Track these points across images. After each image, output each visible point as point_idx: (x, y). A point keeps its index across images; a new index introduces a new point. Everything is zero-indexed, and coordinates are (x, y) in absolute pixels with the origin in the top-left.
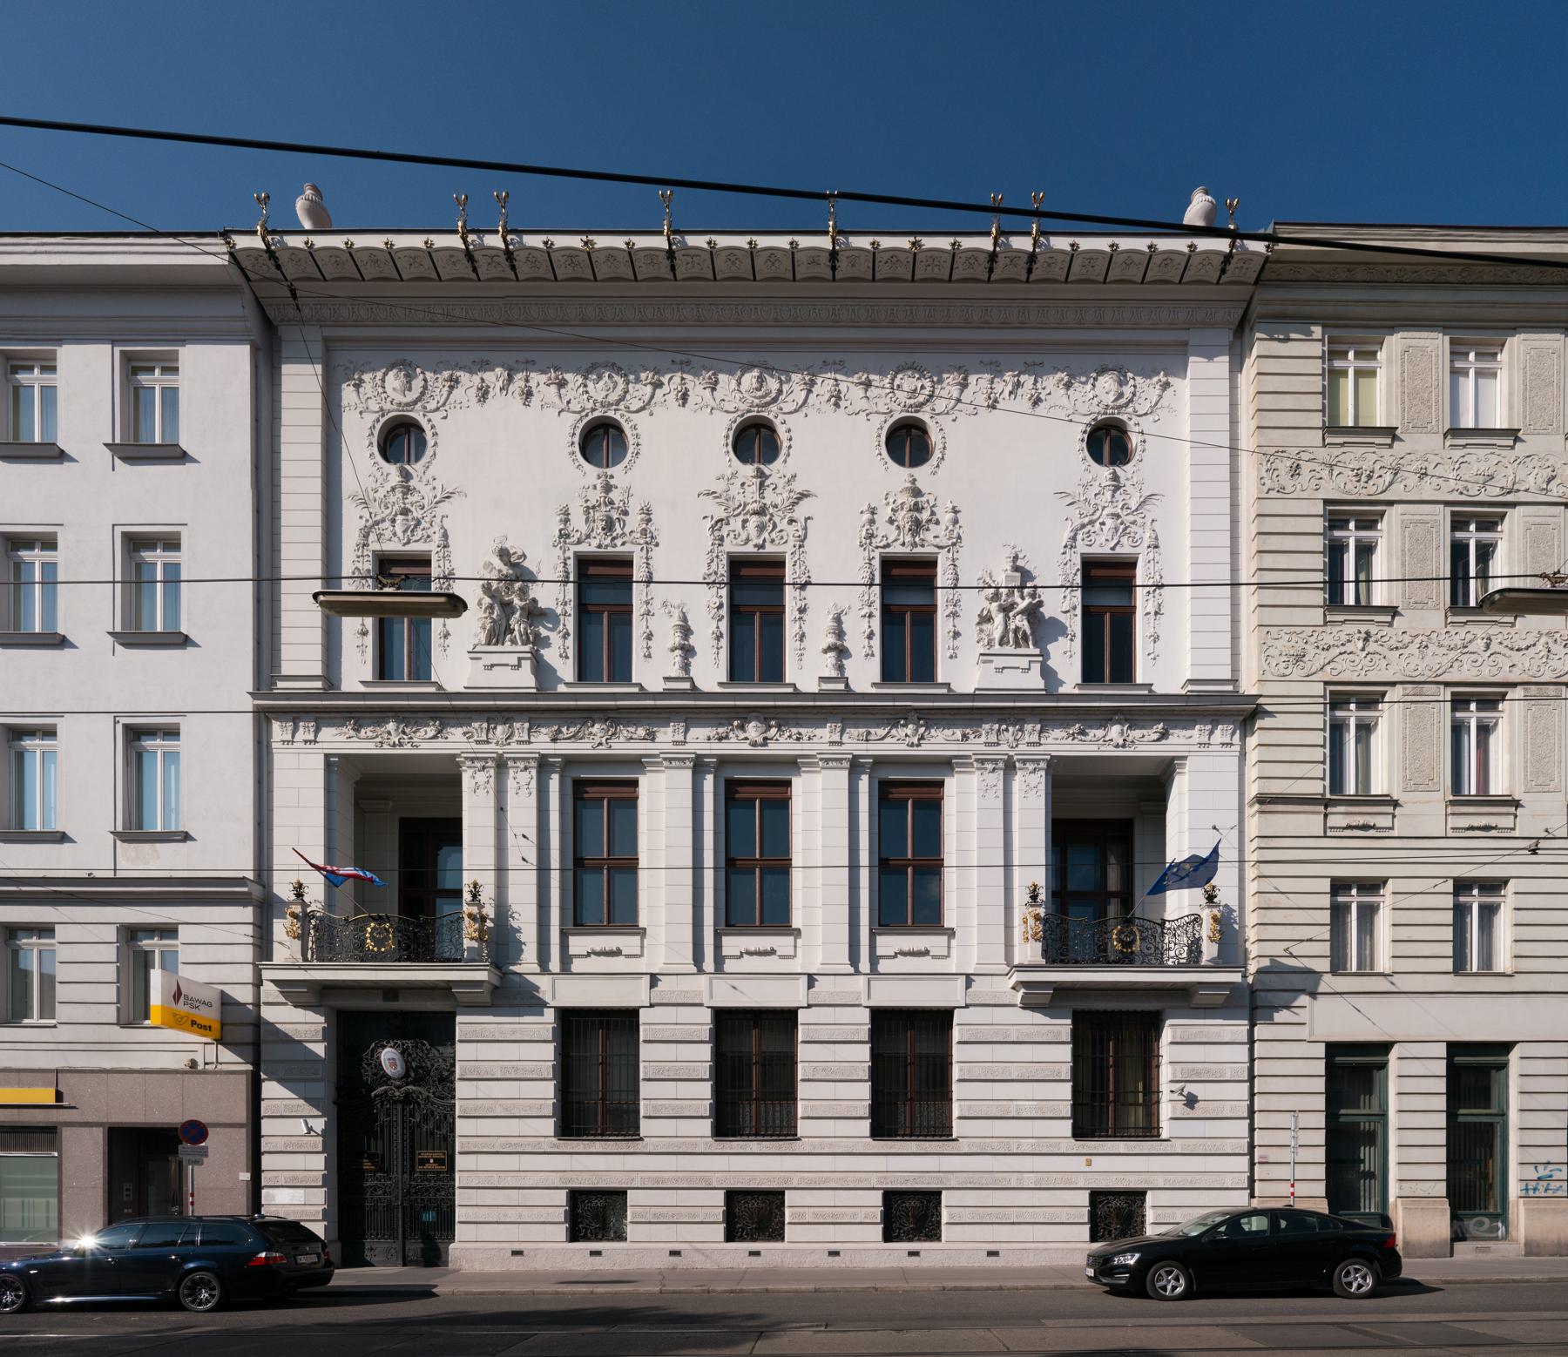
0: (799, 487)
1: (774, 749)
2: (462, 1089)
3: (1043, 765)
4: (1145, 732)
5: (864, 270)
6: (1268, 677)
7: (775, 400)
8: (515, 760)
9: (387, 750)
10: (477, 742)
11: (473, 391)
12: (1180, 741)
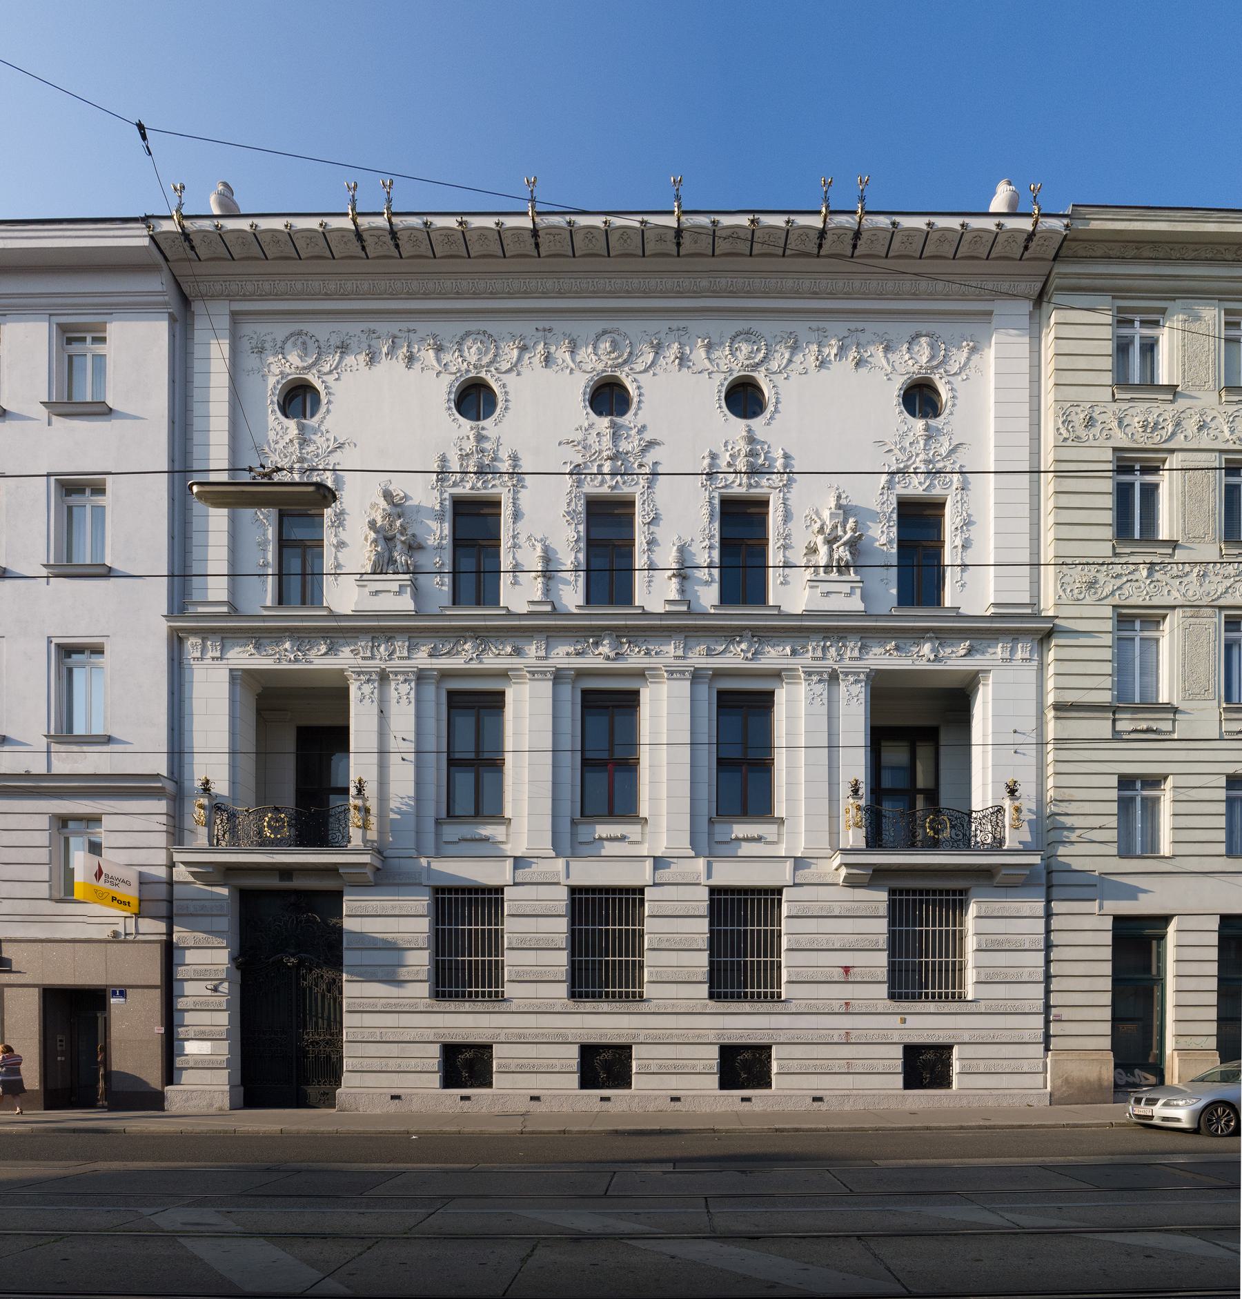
0: (648, 436)
3: (862, 677)
5: (704, 244)
6: (1064, 600)
8: (396, 674)
9: (285, 666)
10: (364, 658)
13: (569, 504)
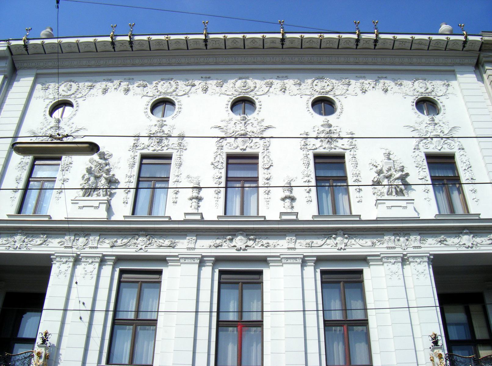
0: (265, 124)
3: (426, 259)
4: (482, 239)
7: (252, 91)
10: (66, 247)
11: (101, 90)
13: (215, 158)
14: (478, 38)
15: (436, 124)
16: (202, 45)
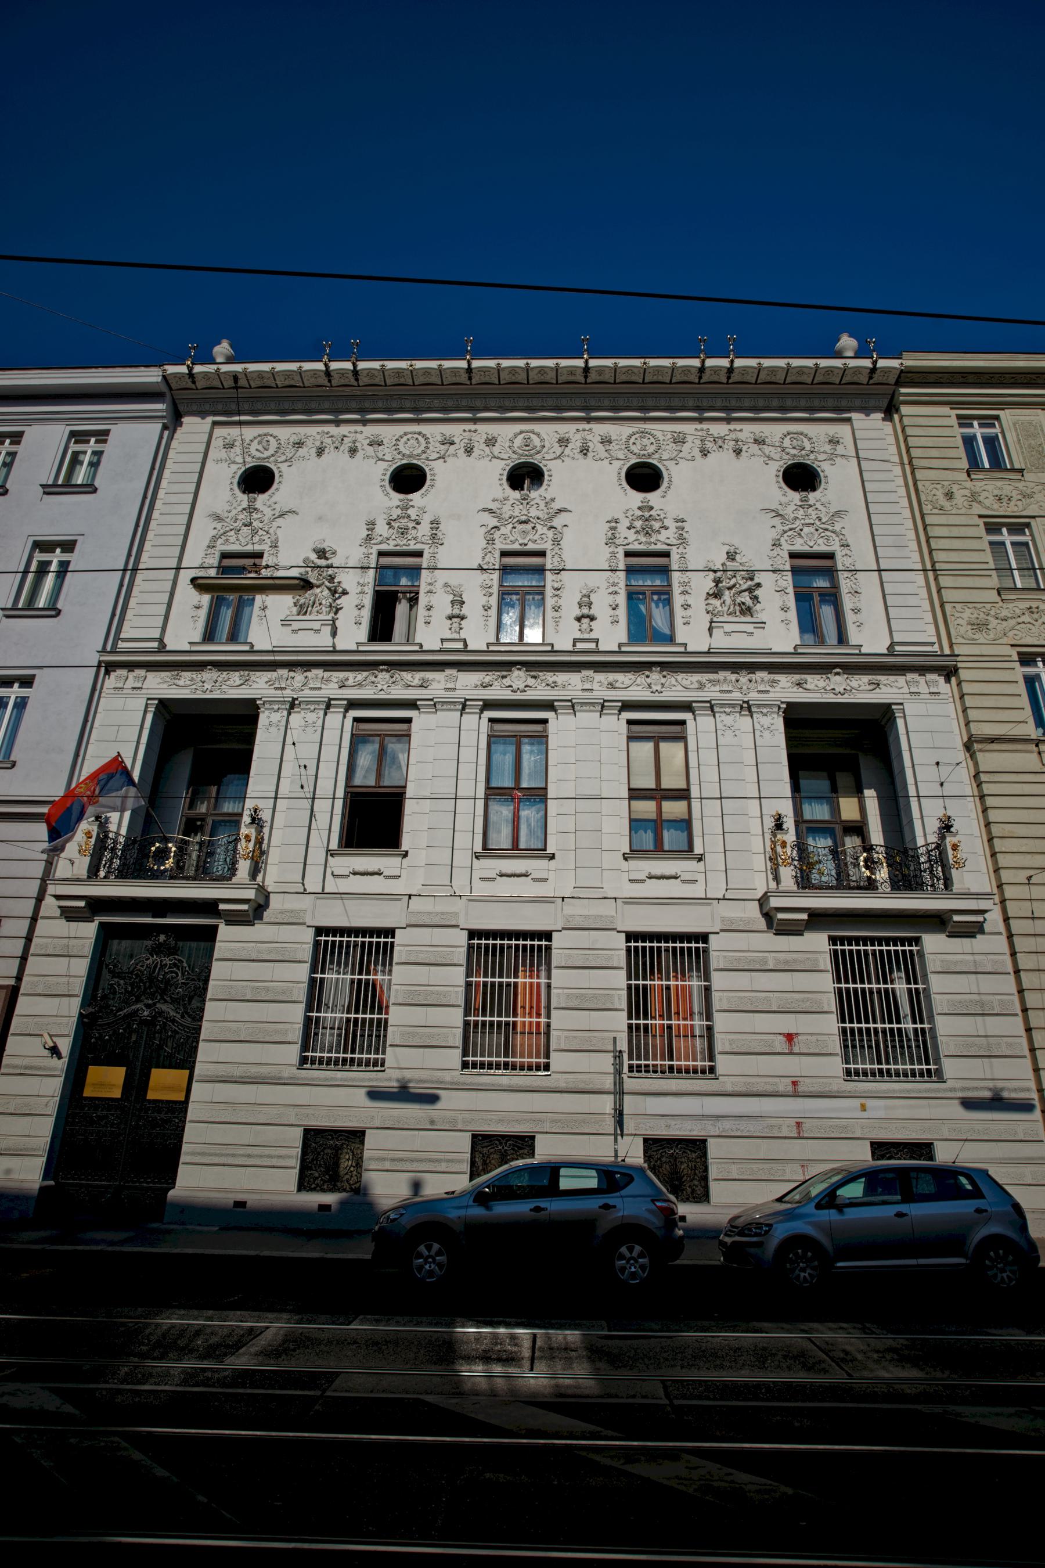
0: (556, 506)
1: (531, 695)
2: (212, 1010)
7: (539, 452)
10: (276, 689)
11: (314, 450)
12: (890, 690)
13: (483, 558)
14: (895, 363)
15: (811, 506)
16: (464, 378)
